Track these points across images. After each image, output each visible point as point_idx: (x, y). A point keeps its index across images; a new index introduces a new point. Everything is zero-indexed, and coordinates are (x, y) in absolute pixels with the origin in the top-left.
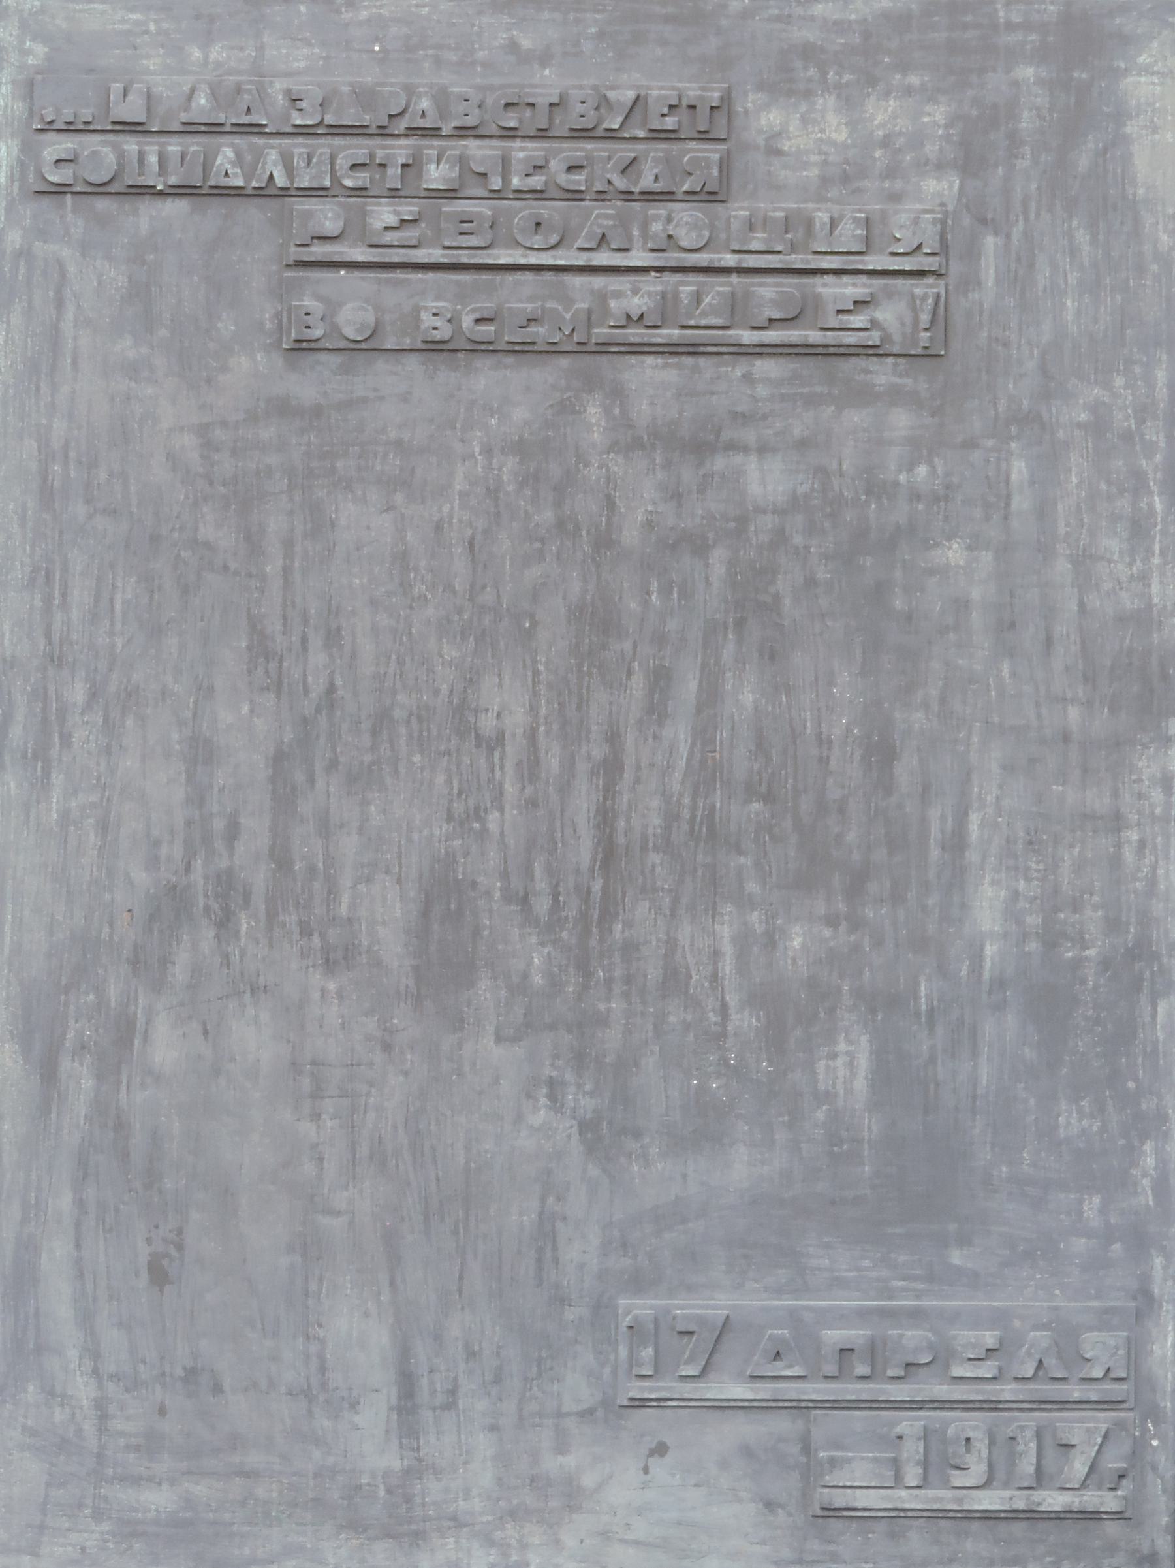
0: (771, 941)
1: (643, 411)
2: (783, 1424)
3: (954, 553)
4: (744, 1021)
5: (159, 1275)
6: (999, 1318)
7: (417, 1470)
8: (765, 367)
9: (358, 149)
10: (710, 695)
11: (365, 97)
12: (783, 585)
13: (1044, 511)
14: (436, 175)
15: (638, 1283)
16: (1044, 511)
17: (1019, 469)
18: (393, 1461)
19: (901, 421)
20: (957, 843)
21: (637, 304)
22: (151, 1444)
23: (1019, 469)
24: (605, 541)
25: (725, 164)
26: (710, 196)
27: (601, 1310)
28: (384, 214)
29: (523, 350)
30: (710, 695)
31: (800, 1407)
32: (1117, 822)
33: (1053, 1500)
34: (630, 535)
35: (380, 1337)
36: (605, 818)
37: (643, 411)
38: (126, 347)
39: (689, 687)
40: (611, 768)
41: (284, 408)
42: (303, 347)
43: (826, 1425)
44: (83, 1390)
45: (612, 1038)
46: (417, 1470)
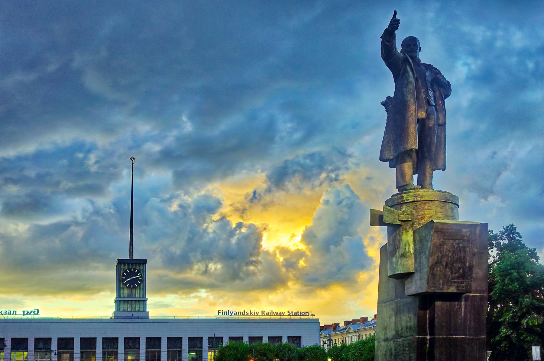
0: (459, 265)
1: (457, 242)
3: (468, 249)
4: (457, 268)
5: (434, 279)
7: (443, 288)
12: (461, 250)
13: (471, 247)
15: (452, 280)
16: (471, 247)
17: (471, 245)
18: (442, 287)
19: (466, 243)
20: (466, 261)
22: (433, 286)
23: (471, 245)
24: (455, 248)
29: (452, 240)
32: (473, 261)
34: (456, 248)
35: (442, 282)
41: (443, 241)
42: (444, 239)
44: (430, 284)
45: (452, 269)
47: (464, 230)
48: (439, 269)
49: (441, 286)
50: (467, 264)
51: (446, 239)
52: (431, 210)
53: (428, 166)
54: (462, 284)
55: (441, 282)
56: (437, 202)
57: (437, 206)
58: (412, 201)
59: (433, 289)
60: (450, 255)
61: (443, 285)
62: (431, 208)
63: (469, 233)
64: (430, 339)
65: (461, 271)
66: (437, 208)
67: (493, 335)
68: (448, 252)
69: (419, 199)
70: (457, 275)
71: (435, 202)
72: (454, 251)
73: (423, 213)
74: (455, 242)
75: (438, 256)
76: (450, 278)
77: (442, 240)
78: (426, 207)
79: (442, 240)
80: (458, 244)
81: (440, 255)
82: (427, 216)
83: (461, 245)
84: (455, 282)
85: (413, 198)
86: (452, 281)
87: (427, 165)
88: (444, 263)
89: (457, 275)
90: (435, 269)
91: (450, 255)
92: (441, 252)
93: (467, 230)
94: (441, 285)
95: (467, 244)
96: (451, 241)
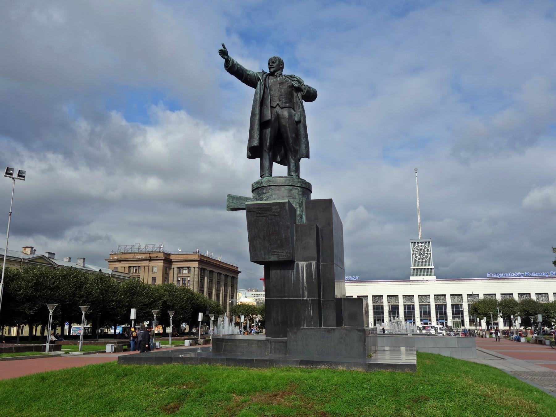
1: (269, 218)
2: (278, 255)
4: (275, 240)
14: (261, 210)
15: (272, 250)
17: (283, 220)
19: (279, 218)
20: (282, 233)
23: (283, 220)
26: (271, 210)
27: (271, 251)
28: (259, 212)
29: (265, 216)
36: (269, 233)
37: (269, 218)
38: (251, 217)
39: (272, 228)
42: (257, 217)
43: (279, 255)
46: (265, 257)
47: (274, 208)
48: (258, 242)
49: (263, 256)
50: (283, 235)
51: (259, 216)
52: (268, 194)
53: (290, 157)
54: (282, 253)
55: (262, 252)
56: (273, 186)
57: (273, 190)
58: (256, 188)
59: (256, 258)
60: (265, 229)
61: (265, 255)
62: (268, 192)
63: (279, 209)
64: (322, 300)
65: (279, 242)
66: (273, 191)
67: (28, 298)
68: (263, 227)
69: (259, 186)
71: (271, 187)
73: (262, 196)
74: (268, 218)
75: (255, 232)
76: (270, 249)
77: (255, 218)
78: (264, 192)
79: (255, 218)
81: (256, 230)
82: (265, 198)
83: (274, 220)
84: (275, 252)
85: (257, 185)
86: (272, 251)
87: (289, 156)
88: (262, 237)
90: (255, 242)
91: (265, 229)
93: (277, 207)
94: (263, 255)
95: (279, 219)
96: (265, 218)
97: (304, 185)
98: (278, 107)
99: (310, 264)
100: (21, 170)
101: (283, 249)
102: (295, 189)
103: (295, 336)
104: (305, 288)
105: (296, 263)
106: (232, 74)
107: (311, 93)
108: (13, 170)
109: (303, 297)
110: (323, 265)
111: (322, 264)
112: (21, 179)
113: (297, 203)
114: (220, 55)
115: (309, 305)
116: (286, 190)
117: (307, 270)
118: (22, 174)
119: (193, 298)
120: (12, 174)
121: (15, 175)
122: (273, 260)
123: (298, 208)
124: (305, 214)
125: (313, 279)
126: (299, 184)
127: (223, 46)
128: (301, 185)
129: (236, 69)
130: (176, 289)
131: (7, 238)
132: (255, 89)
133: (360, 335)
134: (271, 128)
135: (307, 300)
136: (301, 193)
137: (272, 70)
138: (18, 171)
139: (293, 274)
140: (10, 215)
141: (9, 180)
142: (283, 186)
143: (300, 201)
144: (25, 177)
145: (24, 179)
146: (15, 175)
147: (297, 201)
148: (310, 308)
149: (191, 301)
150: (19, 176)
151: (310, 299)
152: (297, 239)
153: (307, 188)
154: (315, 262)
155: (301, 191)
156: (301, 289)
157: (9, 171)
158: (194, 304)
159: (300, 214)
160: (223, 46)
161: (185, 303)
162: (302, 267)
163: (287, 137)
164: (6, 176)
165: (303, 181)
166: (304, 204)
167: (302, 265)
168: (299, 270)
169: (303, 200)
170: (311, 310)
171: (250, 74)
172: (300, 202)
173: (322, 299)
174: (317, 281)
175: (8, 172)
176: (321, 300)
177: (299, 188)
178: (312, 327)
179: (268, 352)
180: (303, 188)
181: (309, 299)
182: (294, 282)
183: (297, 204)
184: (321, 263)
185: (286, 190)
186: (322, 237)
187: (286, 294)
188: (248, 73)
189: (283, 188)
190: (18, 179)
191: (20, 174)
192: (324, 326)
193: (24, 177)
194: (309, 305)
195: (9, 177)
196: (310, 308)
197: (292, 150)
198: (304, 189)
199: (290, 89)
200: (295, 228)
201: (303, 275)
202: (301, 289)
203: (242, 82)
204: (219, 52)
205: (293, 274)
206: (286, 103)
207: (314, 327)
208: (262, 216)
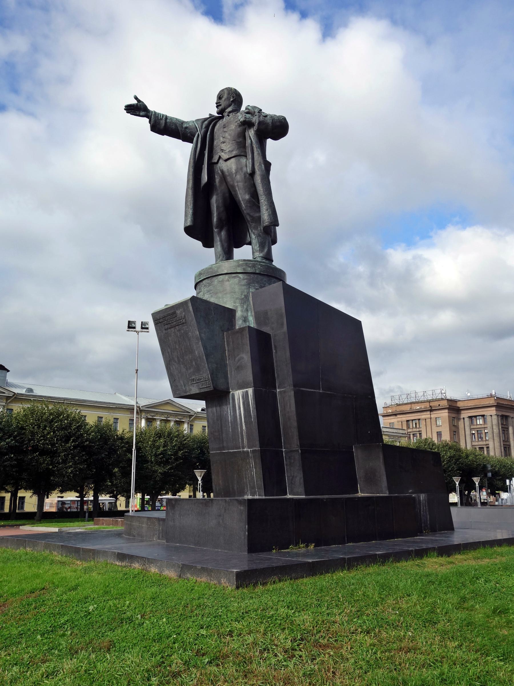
6: (203, 376)
8: (181, 325)
9: (164, 318)
10: (184, 344)
11: (163, 316)
15: (190, 377)
18: (185, 389)
21: (175, 323)
25: (176, 315)
26: (176, 317)
29: (172, 327)
30: (184, 344)
31: (198, 383)
33: (208, 386)
34: (179, 336)
40: (181, 349)
48: (174, 367)
51: (167, 329)
55: (182, 382)
70: (192, 370)
72: (179, 341)
77: (164, 331)
80: (179, 330)
81: (169, 350)
88: (176, 359)
89: (192, 370)
92: (169, 346)
94: (183, 387)
96: (172, 329)
97: (249, 269)
98: (221, 161)
99: (247, 392)
100: (143, 321)
101: (201, 374)
102: (235, 277)
103: (173, 512)
104: (244, 433)
105: (231, 393)
106: (163, 135)
107: (269, 123)
108: (134, 322)
109: (243, 448)
110: (280, 392)
111: (279, 391)
112: (145, 332)
113: (237, 298)
114: (127, 112)
115: (251, 460)
116: (219, 282)
117: (244, 403)
118: (145, 325)
119: (460, 456)
120: (134, 328)
121: (138, 327)
122: (194, 393)
123: (239, 307)
124: (253, 313)
125: (251, 418)
126: (240, 268)
127: (136, 98)
128: (244, 269)
129: (163, 125)
130: (433, 445)
131: (135, 398)
132: (192, 143)
133: (240, 509)
134: (217, 195)
135: (247, 452)
136: (244, 282)
137: (220, 108)
138: (141, 323)
139: (229, 411)
140: (137, 372)
141: (132, 334)
142: (216, 277)
143: (242, 294)
144: (149, 329)
145: (148, 330)
146: (138, 327)
147: (237, 296)
148: (252, 465)
149: (457, 460)
150: (142, 328)
151: (250, 450)
152: (229, 356)
153: (257, 272)
154: (251, 389)
155: (244, 279)
156: (240, 435)
157: (131, 324)
158: (462, 464)
159: (243, 316)
160: (136, 98)
161: (447, 463)
162: (238, 399)
163: (240, 201)
164: (128, 331)
165: (246, 263)
166: (251, 299)
167: (238, 394)
168: (235, 404)
169: (248, 293)
170: (253, 467)
171: (190, 126)
172: (243, 297)
173: (284, 450)
174: (256, 421)
175: (130, 326)
176: (282, 451)
177: (240, 275)
178: (256, 496)
179: (156, 536)
180: (248, 274)
181: (249, 450)
182: (231, 424)
183: (238, 301)
184: (278, 390)
185: (219, 282)
186: (275, 347)
187: (225, 444)
188: (185, 125)
189: (216, 280)
190: (142, 331)
191: (143, 326)
192: (290, 494)
193: (147, 328)
194: (251, 460)
195: (132, 331)
196: (252, 465)
197: (249, 219)
198: (252, 275)
199: (241, 128)
200: (226, 339)
201: (241, 413)
202: (240, 435)
203: (183, 141)
204: (125, 109)
205: (229, 411)
206: (230, 152)
207: (259, 496)
208: (170, 328)
